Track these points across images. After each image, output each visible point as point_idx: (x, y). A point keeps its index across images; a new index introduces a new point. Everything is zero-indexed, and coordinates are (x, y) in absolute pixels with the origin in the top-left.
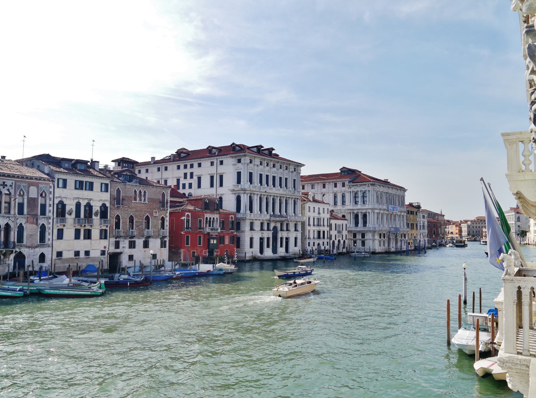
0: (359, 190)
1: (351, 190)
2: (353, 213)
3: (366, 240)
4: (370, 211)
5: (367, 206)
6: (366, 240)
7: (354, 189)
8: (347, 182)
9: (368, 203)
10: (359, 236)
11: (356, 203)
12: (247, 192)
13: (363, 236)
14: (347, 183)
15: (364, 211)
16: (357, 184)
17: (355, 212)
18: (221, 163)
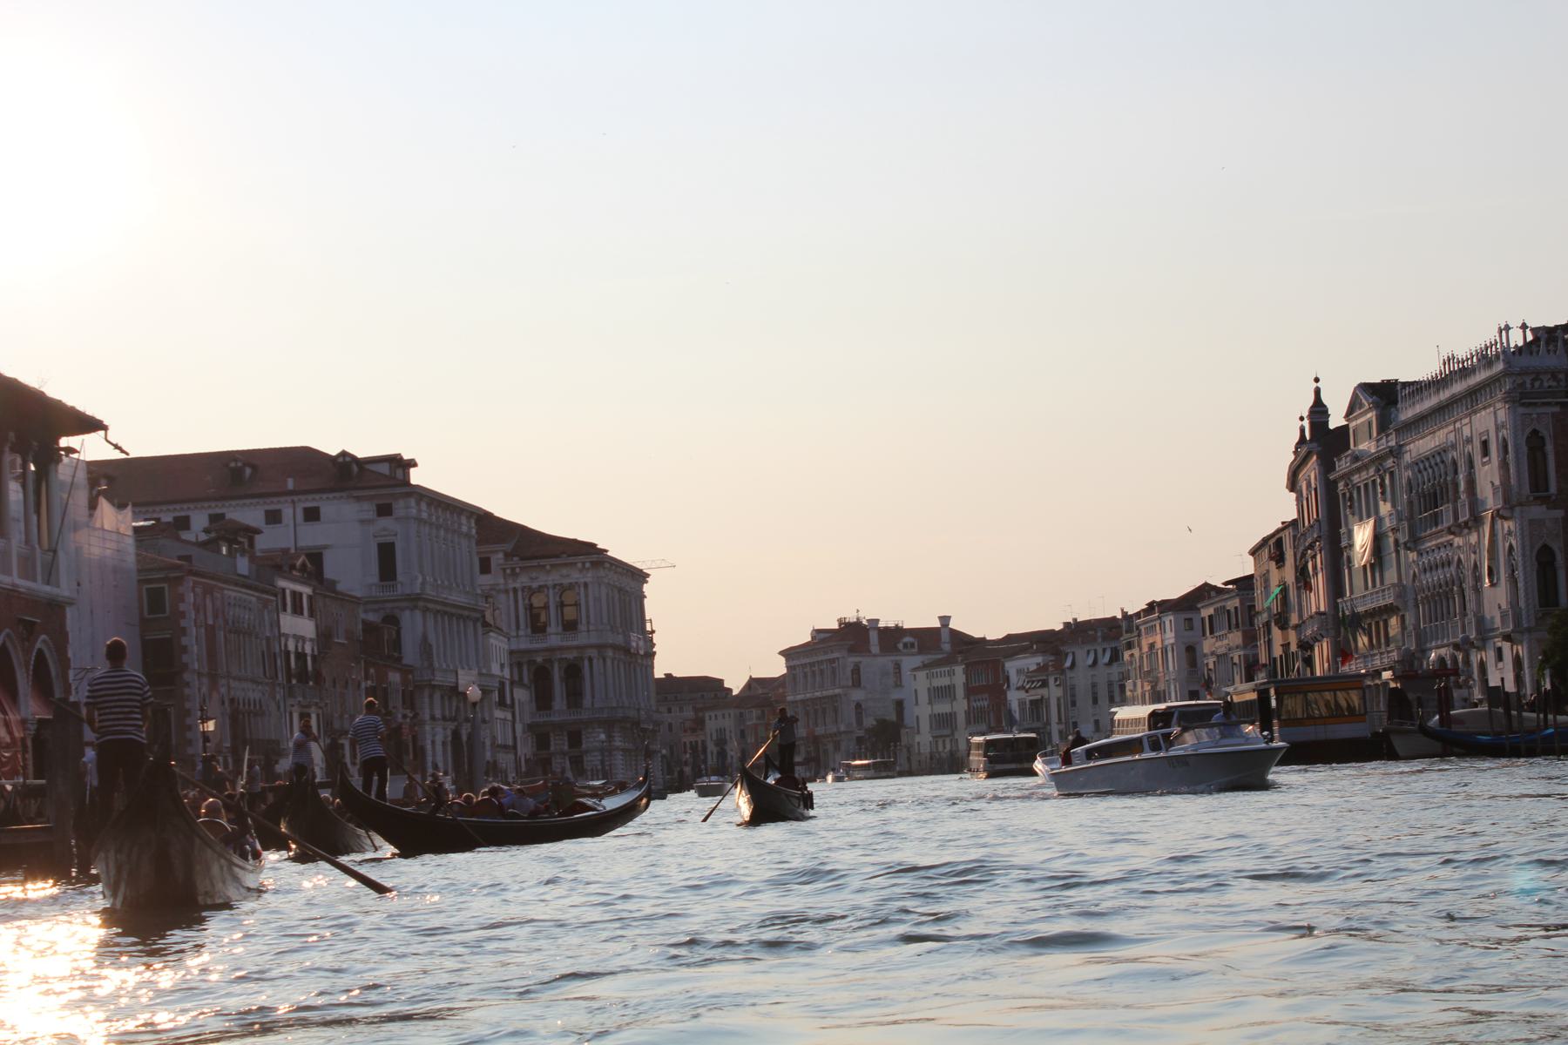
0: (550, 583)
1: (517, 585)
2: (531, 662)
3: (587, 752)
4: (593, 653)
5: (582, 639)
6: (587, 752)
7: (523, 580)
8: (501, 555)
9: (582, 627)
10: (559, 743)
11: (538, 628)
12: (421, 604)
13: (575, 738)
14: (497, 559)
15: (570, 656)
16: (543, 562)
17: (539, 660)
18: (312, 515)
